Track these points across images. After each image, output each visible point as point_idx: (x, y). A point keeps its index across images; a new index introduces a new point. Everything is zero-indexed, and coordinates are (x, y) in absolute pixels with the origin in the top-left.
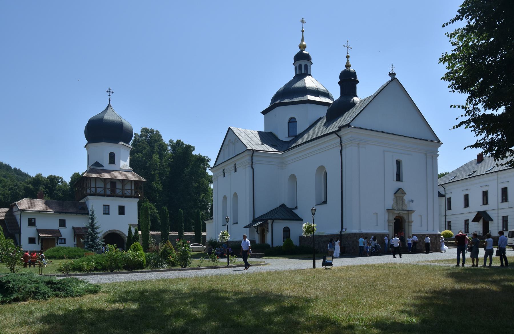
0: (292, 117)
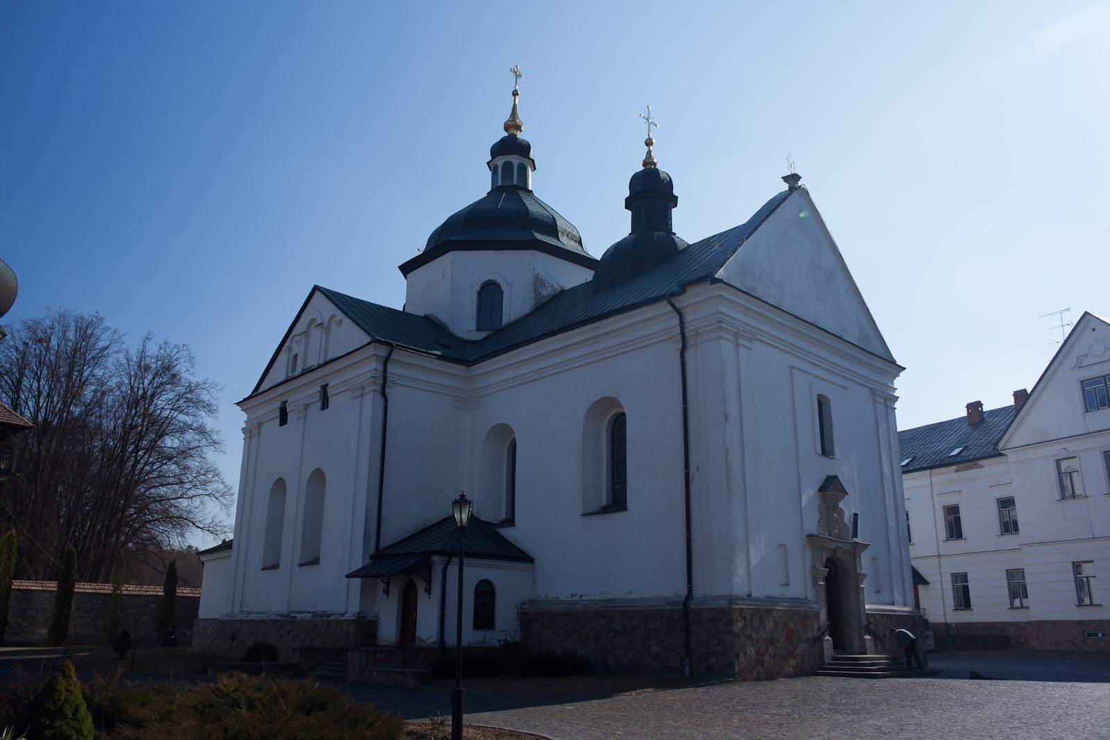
0: (485, 282)
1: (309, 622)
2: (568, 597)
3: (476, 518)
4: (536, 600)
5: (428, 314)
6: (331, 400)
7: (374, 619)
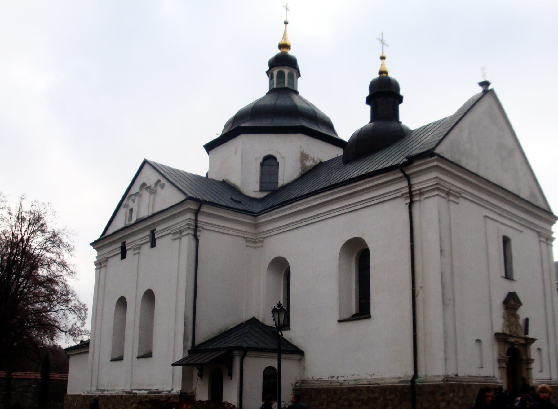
1: (146, 397)
2: (328, 378)
3: (262, 323)
4: (305, 381)
5: (225, 179)
6: (158, 242)
7: (192, 394)
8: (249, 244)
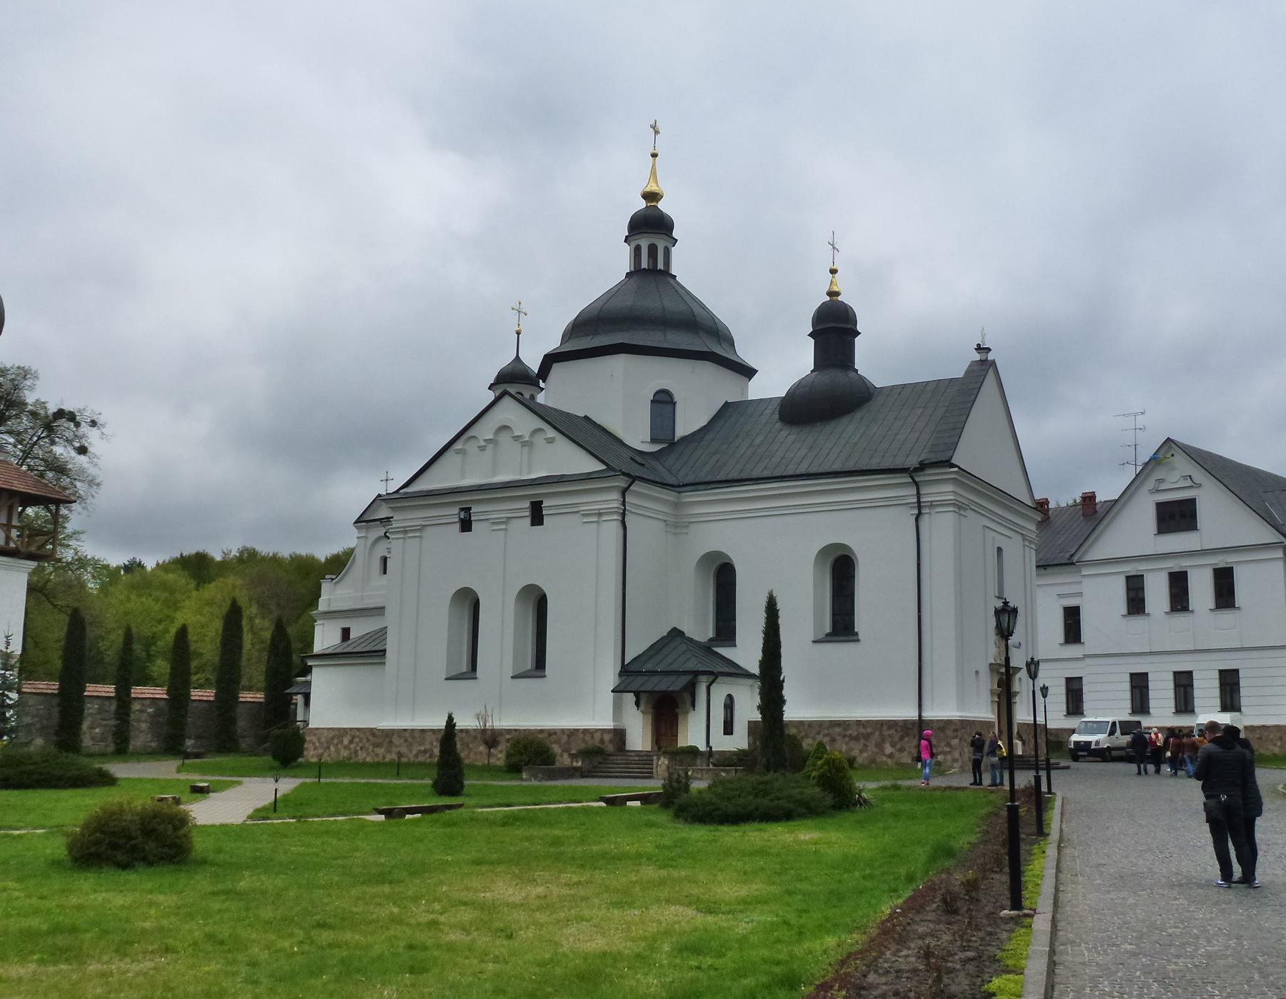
8: (669, 529)
